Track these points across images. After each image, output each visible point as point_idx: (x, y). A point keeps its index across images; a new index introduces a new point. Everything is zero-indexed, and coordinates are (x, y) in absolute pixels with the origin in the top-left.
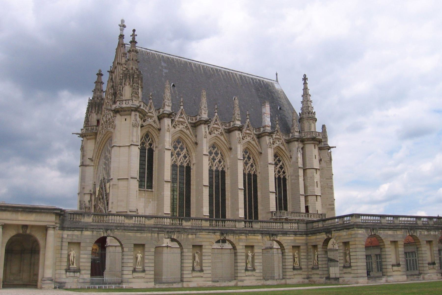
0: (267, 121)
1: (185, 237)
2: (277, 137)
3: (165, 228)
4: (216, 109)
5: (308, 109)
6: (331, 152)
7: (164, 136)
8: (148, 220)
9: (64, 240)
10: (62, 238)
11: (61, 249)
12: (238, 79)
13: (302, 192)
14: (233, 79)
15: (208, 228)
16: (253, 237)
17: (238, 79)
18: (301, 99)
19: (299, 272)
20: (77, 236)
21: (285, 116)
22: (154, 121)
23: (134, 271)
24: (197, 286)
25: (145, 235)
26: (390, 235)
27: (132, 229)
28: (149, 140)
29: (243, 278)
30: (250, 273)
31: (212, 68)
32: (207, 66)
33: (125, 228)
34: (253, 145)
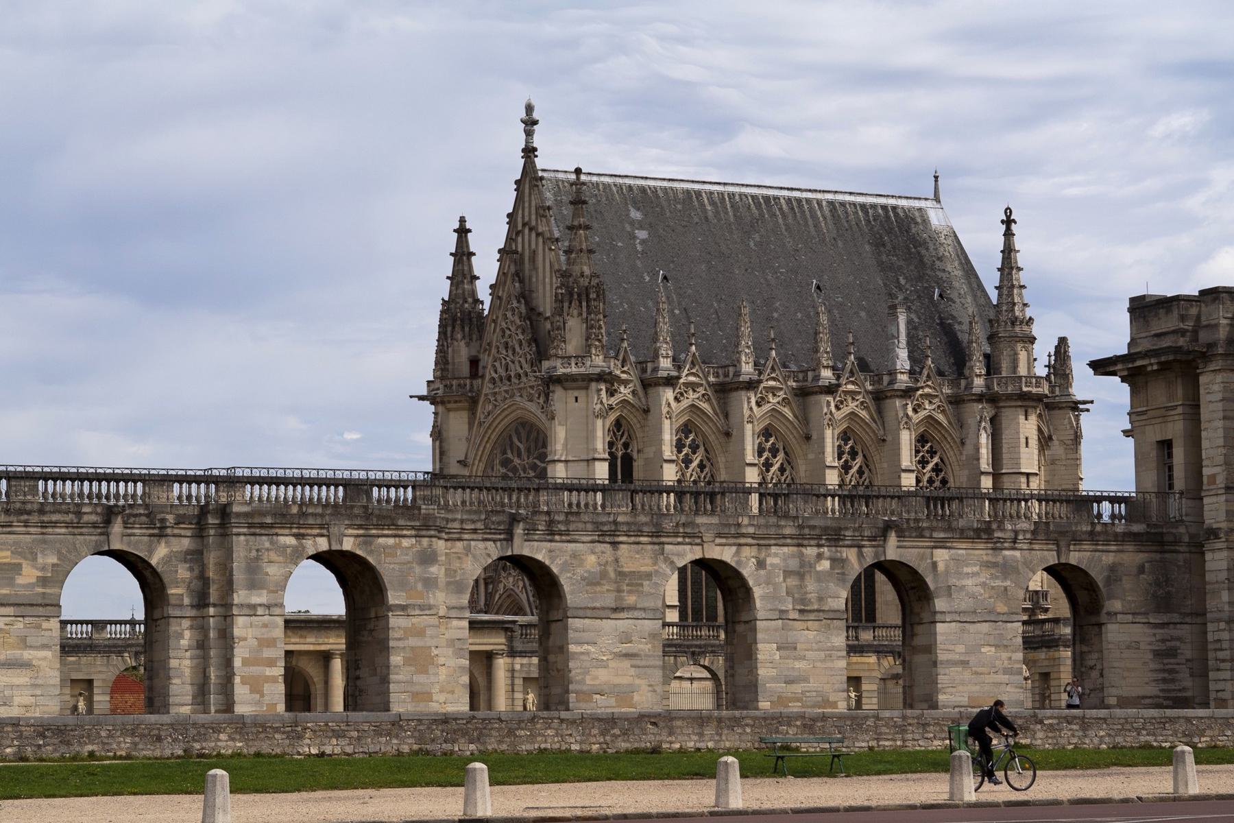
3: (689, 647)
4: (773, 340)
5: (1013, 310)
7: (660, 431)
9: (516, 675)
10: (513, 671)
11: (513, 691)
12: (825, 218)
14: (810, 222)
21: (954, 318)
22: (633, 392)
31: (754, 197)
32: (740, 195)
34: (863, 420)
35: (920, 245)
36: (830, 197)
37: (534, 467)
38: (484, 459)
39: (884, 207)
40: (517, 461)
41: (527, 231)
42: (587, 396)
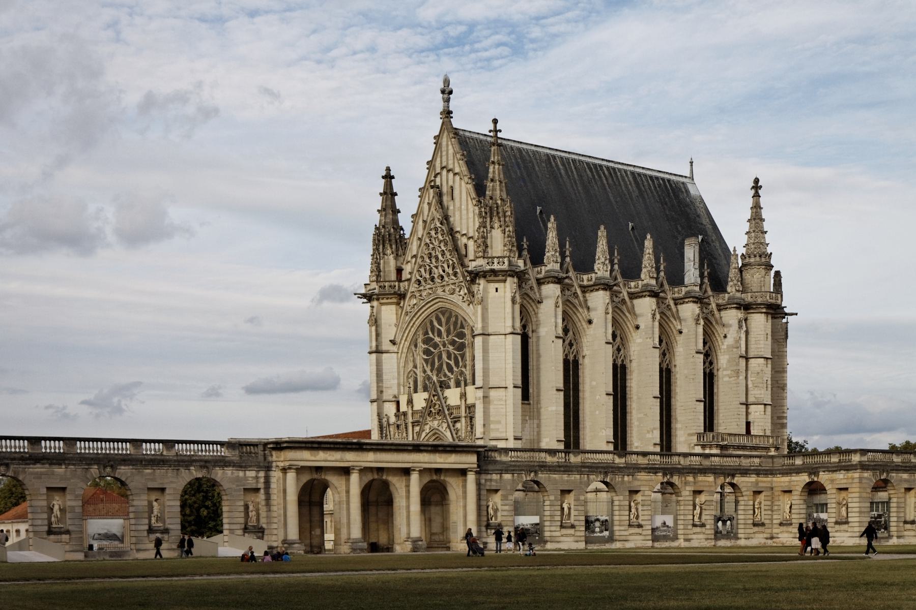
0: (692, 274)
6: (787, 323)
9: (482, 487)
18: (746, 227)
19: (761, 529)
20: (496, 481)
29: (690, 537)
30: (698, 529)
36: (632, 169)
37: (453, 343)
38: (409, 339)
40: (437, 339)
41: (444, 172)
42: (505, 287)
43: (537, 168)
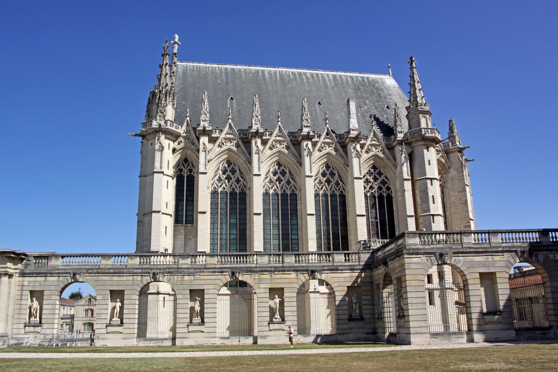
1: (179, 279)
2: (373, 142)
8: (131, 259)
12: (330, 80)
13: (410, 211)
14: (321, 81)
15: (214, 266)
16: (282, 276)
17: (330, 80)
19: (359, 324)
23: (109, 325)
24: (195, 344)
25: (124, 278)
26: (480, 264)
27: (107, 271)
28: (188, 166)
29: (265, 334)
31: (292, 73)
33: (99, 271)
35: (380, 90)
39: (363, 78)
43: (244, 77)
